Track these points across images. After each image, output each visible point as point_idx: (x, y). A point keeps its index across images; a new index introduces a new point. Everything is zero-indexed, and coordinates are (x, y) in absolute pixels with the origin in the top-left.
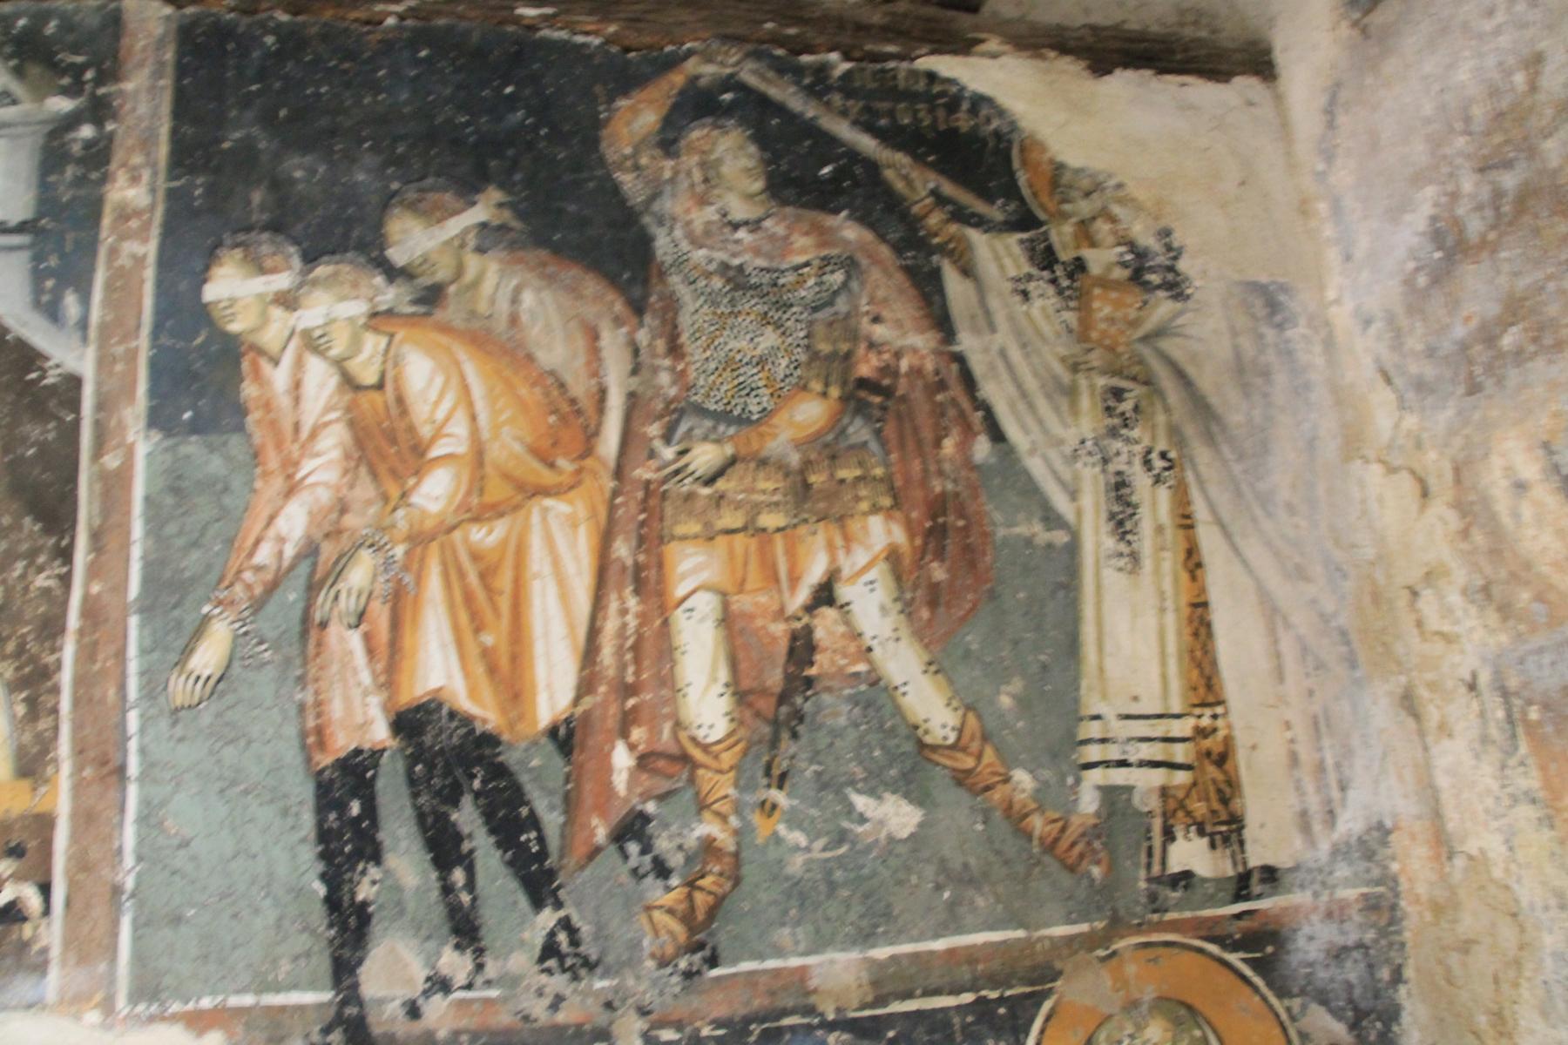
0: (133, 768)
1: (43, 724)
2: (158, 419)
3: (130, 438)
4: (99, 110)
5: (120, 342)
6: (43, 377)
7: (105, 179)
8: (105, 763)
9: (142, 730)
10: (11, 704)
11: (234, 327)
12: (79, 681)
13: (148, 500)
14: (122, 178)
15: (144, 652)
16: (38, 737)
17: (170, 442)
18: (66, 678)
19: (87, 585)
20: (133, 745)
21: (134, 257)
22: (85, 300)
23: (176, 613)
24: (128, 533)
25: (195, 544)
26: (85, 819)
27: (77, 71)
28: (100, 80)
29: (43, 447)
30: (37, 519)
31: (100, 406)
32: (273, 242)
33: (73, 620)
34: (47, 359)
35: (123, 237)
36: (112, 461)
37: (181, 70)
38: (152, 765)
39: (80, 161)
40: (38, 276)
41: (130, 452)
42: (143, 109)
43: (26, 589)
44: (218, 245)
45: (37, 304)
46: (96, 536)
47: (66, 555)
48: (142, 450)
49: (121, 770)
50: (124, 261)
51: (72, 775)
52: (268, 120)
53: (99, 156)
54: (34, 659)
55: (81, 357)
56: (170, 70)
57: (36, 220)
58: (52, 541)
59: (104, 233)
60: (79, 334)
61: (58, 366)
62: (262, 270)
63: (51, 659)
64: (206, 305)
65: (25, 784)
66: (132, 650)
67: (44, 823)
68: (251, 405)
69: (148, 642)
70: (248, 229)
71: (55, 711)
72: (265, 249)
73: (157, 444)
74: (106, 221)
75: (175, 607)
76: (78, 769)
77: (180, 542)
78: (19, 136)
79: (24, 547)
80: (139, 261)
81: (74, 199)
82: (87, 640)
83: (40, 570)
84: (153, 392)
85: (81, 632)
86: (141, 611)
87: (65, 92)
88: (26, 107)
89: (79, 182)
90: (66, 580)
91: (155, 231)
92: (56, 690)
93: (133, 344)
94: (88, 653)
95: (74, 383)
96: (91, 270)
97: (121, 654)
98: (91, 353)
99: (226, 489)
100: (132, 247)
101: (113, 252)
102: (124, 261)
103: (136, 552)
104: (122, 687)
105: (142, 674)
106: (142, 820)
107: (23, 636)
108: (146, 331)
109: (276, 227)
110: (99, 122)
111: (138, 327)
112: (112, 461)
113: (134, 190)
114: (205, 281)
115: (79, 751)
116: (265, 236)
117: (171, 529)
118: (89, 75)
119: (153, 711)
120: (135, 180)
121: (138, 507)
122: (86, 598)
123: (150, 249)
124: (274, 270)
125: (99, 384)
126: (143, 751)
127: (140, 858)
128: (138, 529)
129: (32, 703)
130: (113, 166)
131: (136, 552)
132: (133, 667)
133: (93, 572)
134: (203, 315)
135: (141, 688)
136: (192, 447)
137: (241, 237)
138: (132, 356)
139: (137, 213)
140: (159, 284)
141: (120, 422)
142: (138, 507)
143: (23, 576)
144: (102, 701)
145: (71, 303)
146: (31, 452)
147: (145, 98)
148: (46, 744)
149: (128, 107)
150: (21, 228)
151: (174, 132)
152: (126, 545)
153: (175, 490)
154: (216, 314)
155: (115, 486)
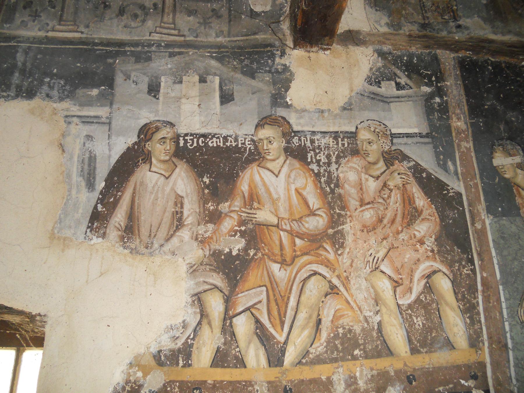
0: (510, 345)
1: (476, 327)
2: (489, 210)
3: (483, 217)
4: (440, 92)
5: (471, 180)
6: (449, 193)
7: (448, 118)
8: (500, 342)
9: (511, 331)
10: (465, 319)
11: (507, 176)
12: (485, 310)
13: (493, 241)
14: (454, 119)
15: (506, 299)
16: (475, 331)
17: (496, 220)
18: (481, 308)
19: (481, 274)
20: (508, 335)
21: (466, 147)
22: (455, 164)
23: (516, 285)
24: (491, 253)
25: (515, 259)
26: (496, 365)
27: (429, 77)
28: (437, 81)
29: (454, 220)
30: (458, 248)
31: (470, 205)
32: (512, 144)
33: (480, 287)
34: (448, 186)
35: (460, 141)
36: (479, 226)
37: (464, 79)
38: (517, 343)
39: (438, 111)
40: (437, 155)
41: (484, 222)
42: (455, 92)
43: (461, 274)
44: (493, 145)
45: (439, 164)
46: (479, 254)
47: (471, 261)
48: (487, 222)
49: (506, 345)
50: (463, 149)
51: (488, 348)
52: (498, 99)
53: (444, 109)
54: (469, 301)
55: (459, 186)
56: (460, 78)
57: (431, 133)
58: (465, 256)
59: (454, 139)
60: (455, 177)
61: (452, 189)
62: (511, 155)
63: (475, 301)
64: (495, 167)
65: (473, 350)
66: (503, 299)
67: (482, 365)
68: (521, 206)
69: (508, 296)
70: (502, 139)
71: (480, 322)
72: (509, 147)
73: (492, 220)
74: (454, 134)
75: (514, 282)
76: (490, 344)
77: (510, 258)
78: (416, 101)
79: (457, 258)
80: (469, 149)
81: (440, 125)
82: (485, 294)
83: (464, 267)
84: (486, 201)
85: (483, 291)
86: (502, 284)
87: (427, 85)
88: (415, 89)
89: (440, 119)
90: (474, 271)
91: (471, 139)
92: (478, 313)
93: (476, 181)
94: (487, 299)
95: (459, 195)
96: (455, 152)
97: (499, 300)
98: (462, 183)
99: (519, 238)
100: (464, 144)
101: (459, 146)
102: (463, 149)
103: (495, 261)
104: (501, 313)
105: (507, 308)
106: (516, 366)
107: (464, 292)
108: (478, 176)
109: (511, 139)
110: (441, 97)
111: (476, 174)
112: (479, 226)
113: (459, 123)
114: (493, 158)
115: (490, 338)
116: (508, 142)
117: (505, 253)
118: (434, 79)
119: (513, 323)
120: (459, 119)
121: (491, 244)
122: (482, 278)
123: (471, 144)
124: (514, 155)
125: (467, 196)
126: (512, 338)
127: (517, 380)
128: (494, 254)
129: (471, 318)
130: (450, 114)
131: (495, 261)
132: (504, 305)
133: (482, 269)
134: (495, 171)
135: (508, 314)
136: (505, 221)
137: (500, 142)
138: (476, 185)
139: (463, 132)
140: (477, 158)
141: (478, 210)
142: (491, 244)
143: (459, 269)
144: (495, 318)
145: (450, 163)
146: (451, 221)
147: (454, 87)
148: (479, 334)
149: (450, 91)
150: (427, 136)
151: (468, 101)
152: (491, 258)
153: (503, 238)
154: (499, 170)
155: (481, 234)
